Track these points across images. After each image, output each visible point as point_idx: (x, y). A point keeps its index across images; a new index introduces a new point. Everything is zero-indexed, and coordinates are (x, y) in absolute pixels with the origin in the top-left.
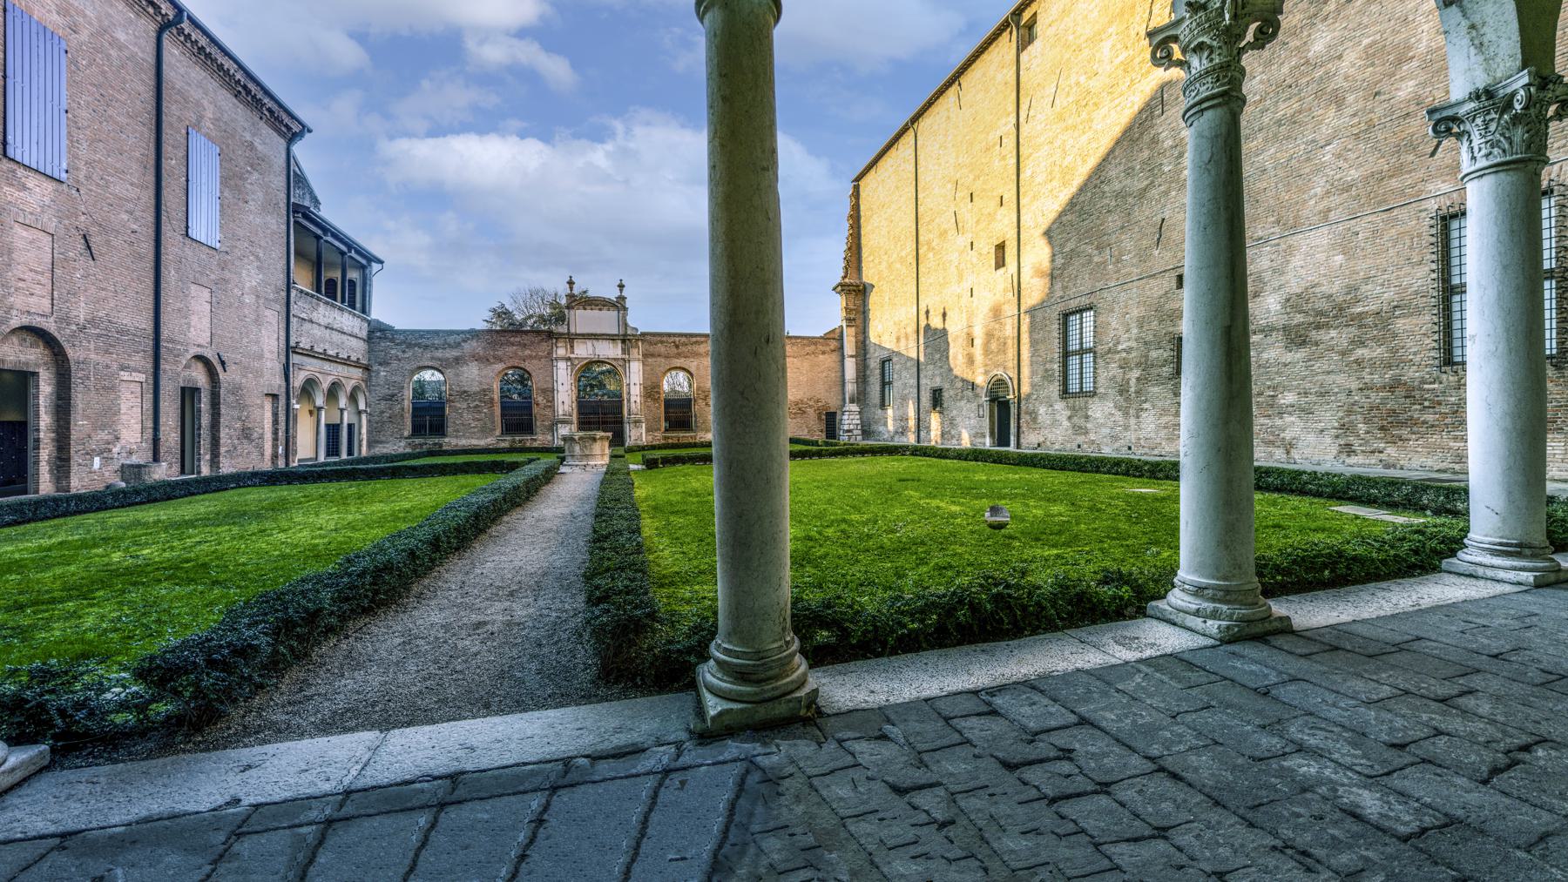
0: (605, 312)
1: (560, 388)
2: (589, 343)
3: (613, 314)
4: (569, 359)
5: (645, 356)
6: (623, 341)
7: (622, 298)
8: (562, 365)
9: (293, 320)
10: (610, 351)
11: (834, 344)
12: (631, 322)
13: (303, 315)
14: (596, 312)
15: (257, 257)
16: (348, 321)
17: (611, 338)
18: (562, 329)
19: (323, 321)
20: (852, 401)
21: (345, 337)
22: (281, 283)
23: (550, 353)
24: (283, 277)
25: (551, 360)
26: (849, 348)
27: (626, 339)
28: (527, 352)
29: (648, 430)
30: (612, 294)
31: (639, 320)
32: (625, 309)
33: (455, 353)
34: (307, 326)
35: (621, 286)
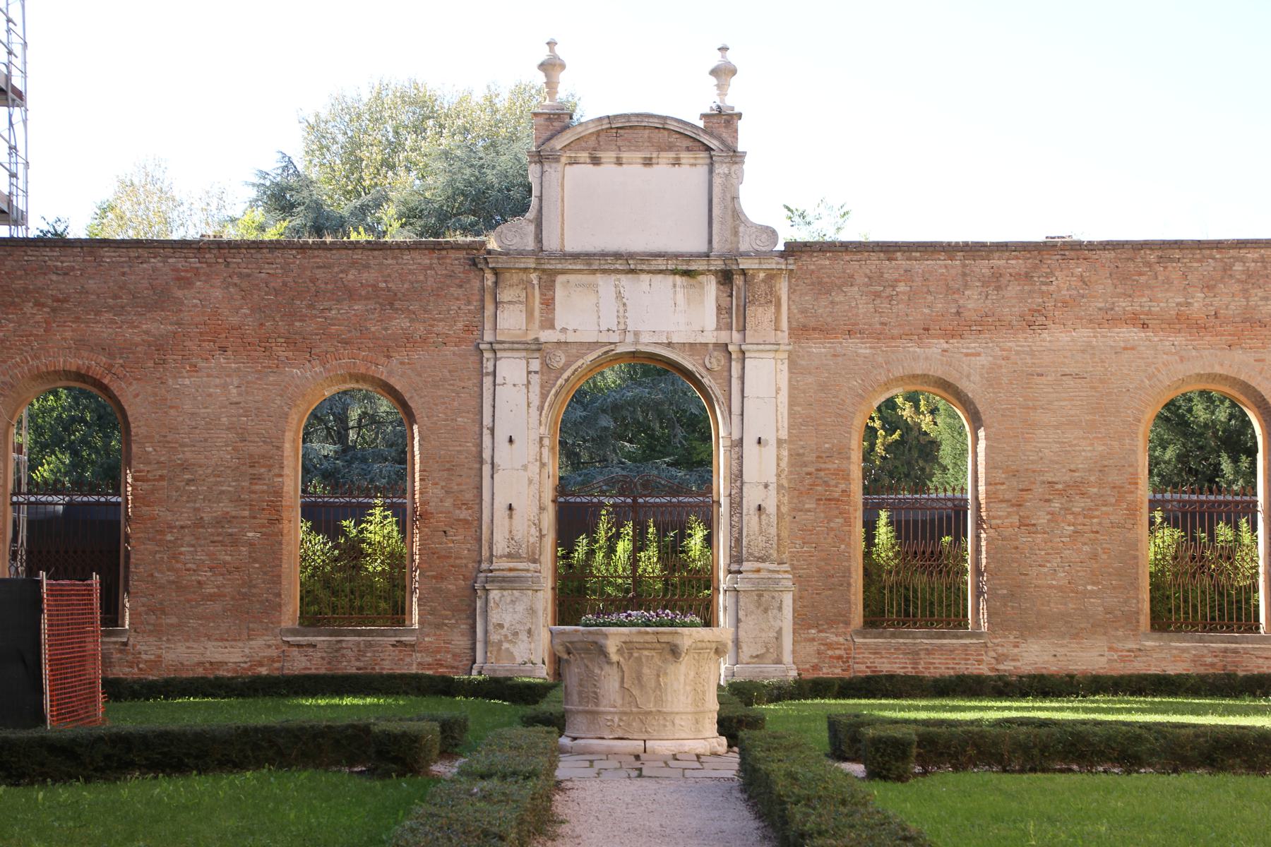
0: (662, 170)
1: (503, 454)
2: (606, 284)
4: (537, 347)
5: (800, 331)
6: (726, 277)
7: (724, 120)
8: (512, 369)
10: (673, 318)
14: (633, 173)
17: (683, 268)
23: (474, 328)
25: (479, 355)
28: (400, 323)
29: (802, 622)
32: (735, 157)
33: (155, 326)
35: (723, 73)
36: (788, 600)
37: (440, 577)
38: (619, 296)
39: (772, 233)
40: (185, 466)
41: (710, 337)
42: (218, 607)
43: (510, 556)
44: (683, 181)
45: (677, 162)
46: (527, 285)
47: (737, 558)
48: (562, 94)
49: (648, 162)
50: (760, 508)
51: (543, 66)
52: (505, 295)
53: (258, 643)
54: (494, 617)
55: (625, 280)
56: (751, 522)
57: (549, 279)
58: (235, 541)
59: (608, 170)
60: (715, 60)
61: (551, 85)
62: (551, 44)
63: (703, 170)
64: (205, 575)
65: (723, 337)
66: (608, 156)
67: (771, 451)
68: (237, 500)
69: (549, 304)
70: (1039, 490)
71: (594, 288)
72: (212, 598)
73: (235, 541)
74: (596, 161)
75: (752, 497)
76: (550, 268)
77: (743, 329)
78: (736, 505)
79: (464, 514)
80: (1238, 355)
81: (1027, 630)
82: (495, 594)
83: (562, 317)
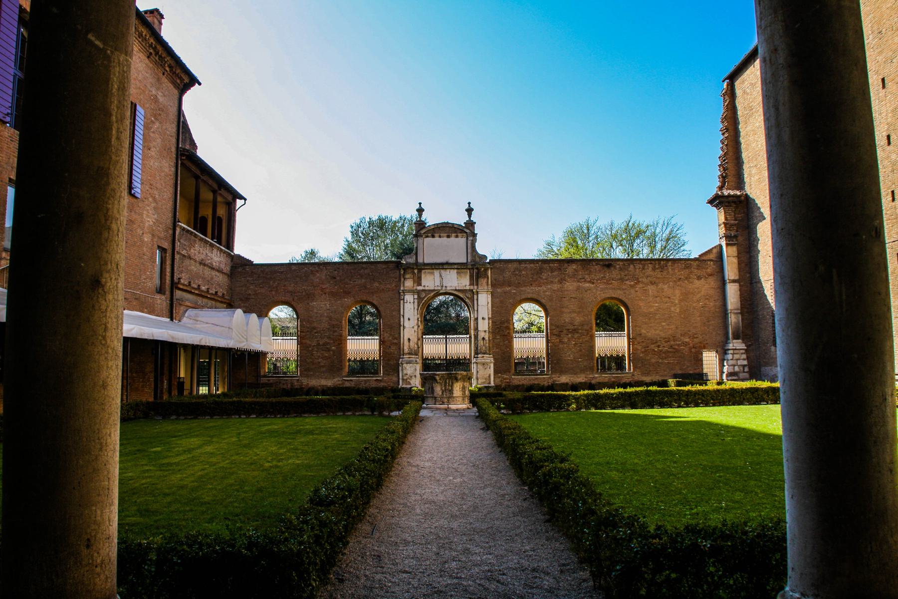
0: (453, 239)
1: (407, 324)
2: (437, 273)
3: (461, 241)
7: (470, 224)
8: (409, 298)
9: (177, 257)
11: (711, 267)
12: (482, 248)
13: (184, 252)
14: (444, 240)
15: (154, 199)
16: (217, 258)
17: (460, 267)
18: (411, 260)
19: (199, 258)
20: (736, 337)
21: (214, 273)
22: (169, 222)
24: (170, 215)
26: (731, 270)
27: (477, 267)
28: (376, 284)
30: (461, 219)
31: (489, 247)
32: (474, 235)
34: (187, 262)
35: (470, 211)
36: (492, 365)
37: (389, 360)
38: (441, 276)
39: (485, 257)
40: (314, 328)
41: (468, 288)
42: (324, 369)
43: (409, 354)
44: (460, 242)
45: (457, 237)
46: (414, 273)
47: (476, 353)
48: (423, 218)
49: (448, 237)
50: (483, 339)
51: (418, 210)
52: (407, 276)
53: (336, 380)
54: (405, 372)
55: (442, 271)
56: (481, 343)
57: (420, 271)
58: (329, 350)
59: (437, 239)
60: (467, 207)
61: (420, 215)
62: (420, 204)
63: (464, 240)
64: (320, 360)
65: (472, 287)
66: (436, 235)
67: (487, 321)
68: (329, 338)
69: (420, 278)
70: (565, 331)
71: (433, 273)
72: (323, 367)
73: (329, 350)
74: (433, 236)
75: (481, 335)
76: (419, 268)
77: (477, 285)
78: (476, 337)
79: (395, 341)
80: (619, 292)
81: (562, 372)
82: (405, 365)
83: (424, 282)
